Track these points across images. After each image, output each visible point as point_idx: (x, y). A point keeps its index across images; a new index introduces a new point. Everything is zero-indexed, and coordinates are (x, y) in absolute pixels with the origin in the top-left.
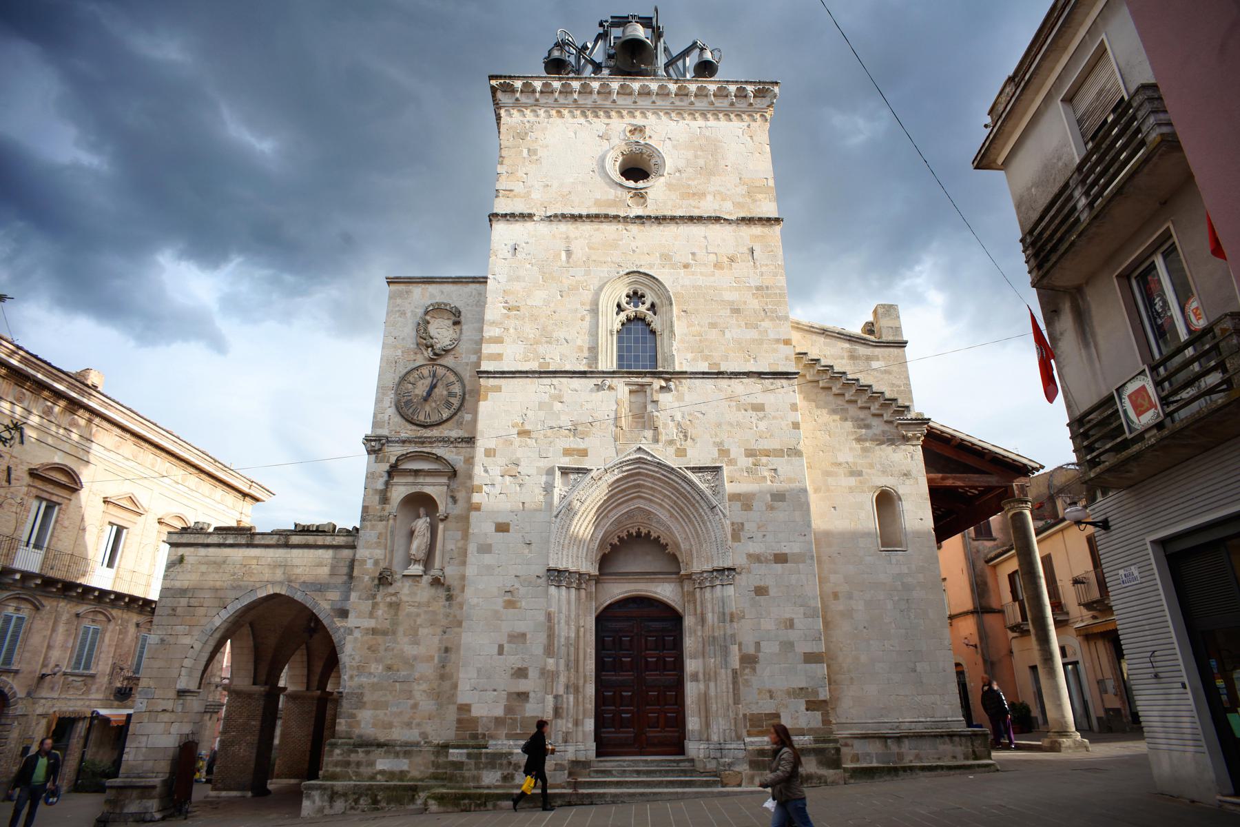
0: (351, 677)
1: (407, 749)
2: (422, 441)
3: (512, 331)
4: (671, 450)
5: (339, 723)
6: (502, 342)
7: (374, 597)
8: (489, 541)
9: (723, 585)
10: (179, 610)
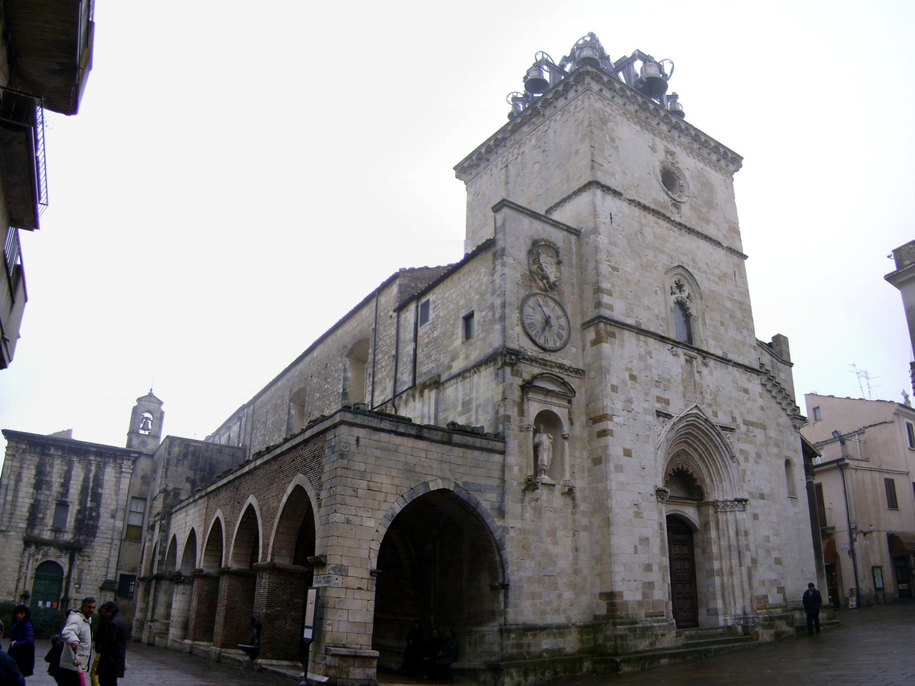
1: (561, 629)
2: (544, 363)
8: (621, 463)
10: (360, 491)
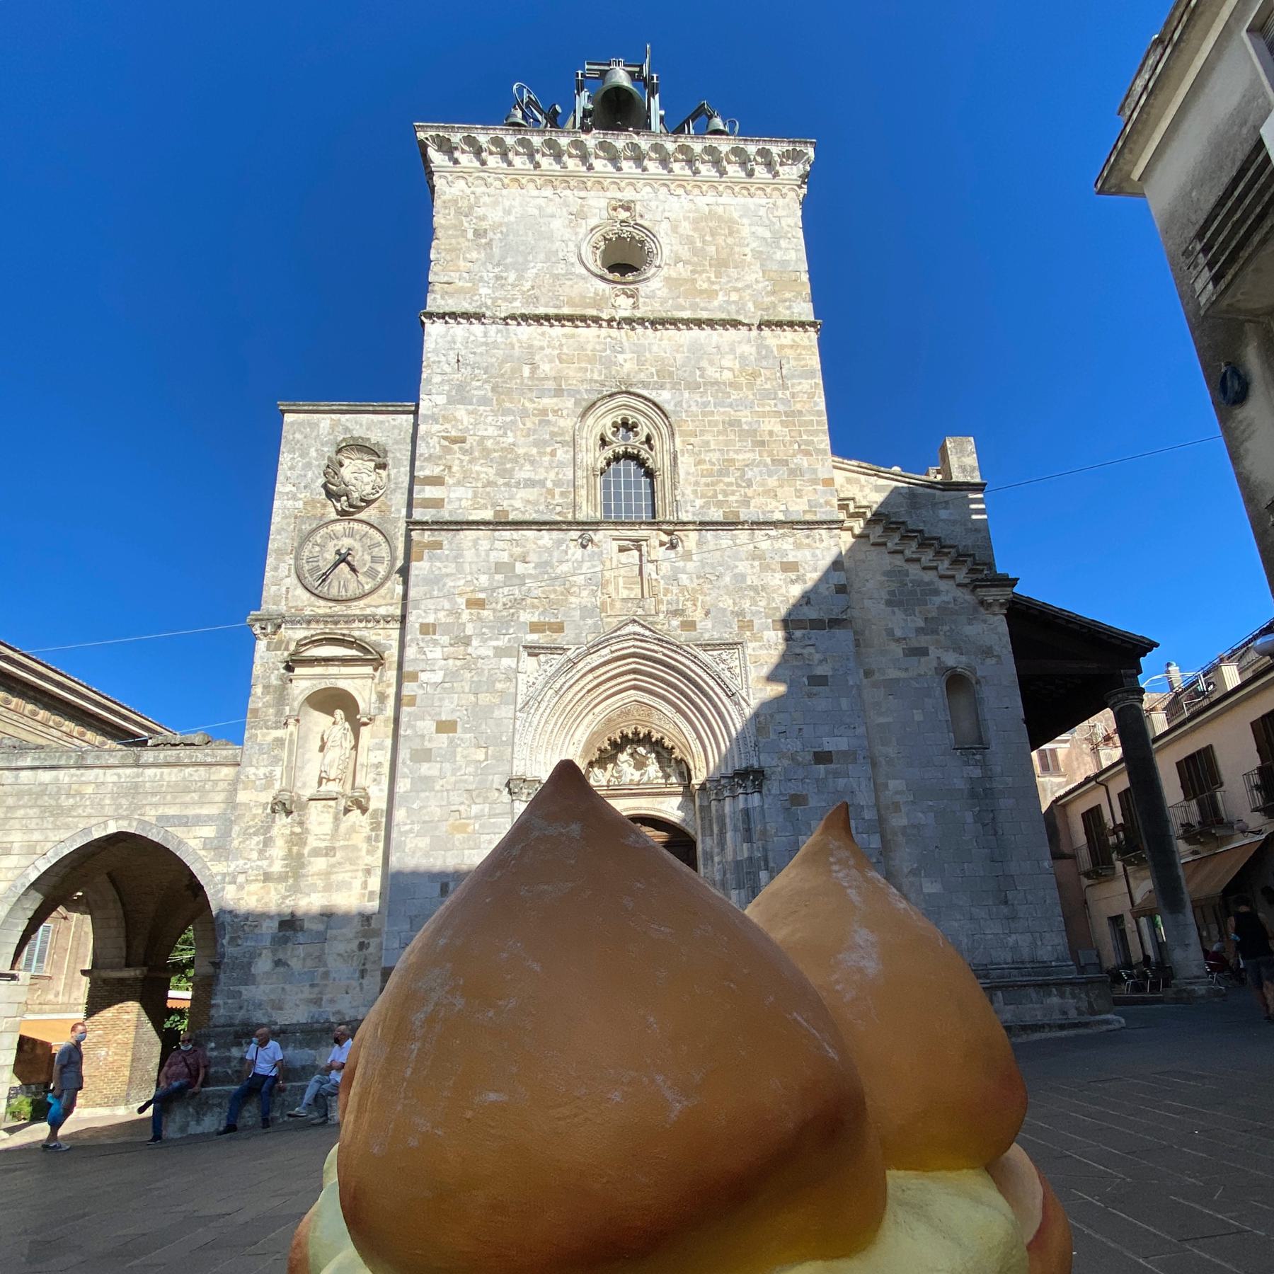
0: (233, 940)
2: (334, 619)
3: (455, 469)
4: (675, 622)
5: (214, 1005)
6: (442, 484)
7: (268, 829)
8: (428, 745)
9: (747, 794)
